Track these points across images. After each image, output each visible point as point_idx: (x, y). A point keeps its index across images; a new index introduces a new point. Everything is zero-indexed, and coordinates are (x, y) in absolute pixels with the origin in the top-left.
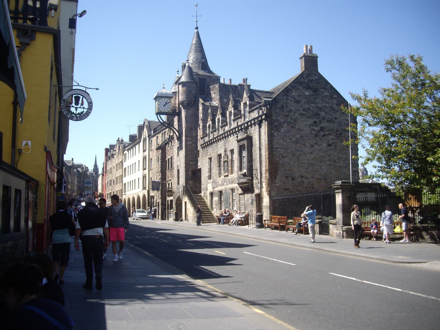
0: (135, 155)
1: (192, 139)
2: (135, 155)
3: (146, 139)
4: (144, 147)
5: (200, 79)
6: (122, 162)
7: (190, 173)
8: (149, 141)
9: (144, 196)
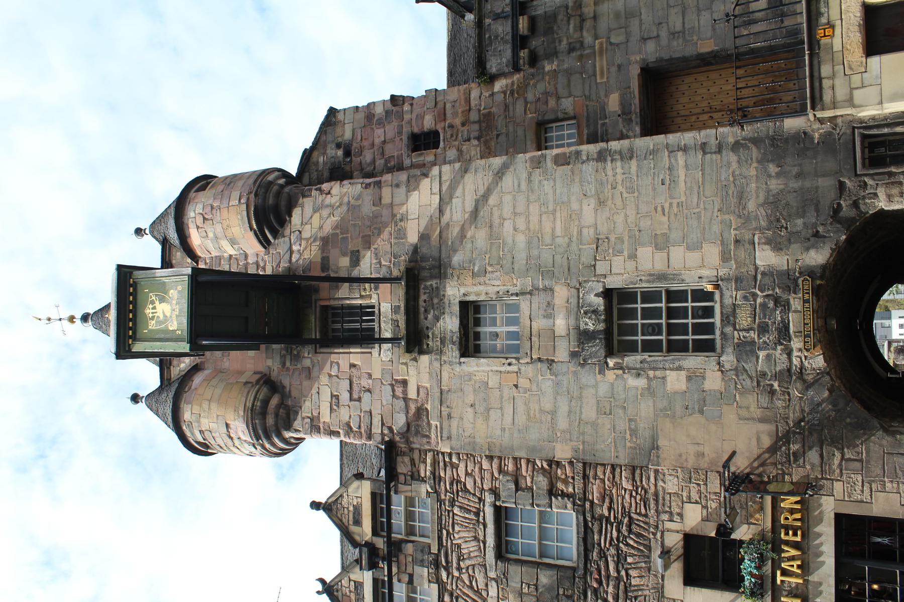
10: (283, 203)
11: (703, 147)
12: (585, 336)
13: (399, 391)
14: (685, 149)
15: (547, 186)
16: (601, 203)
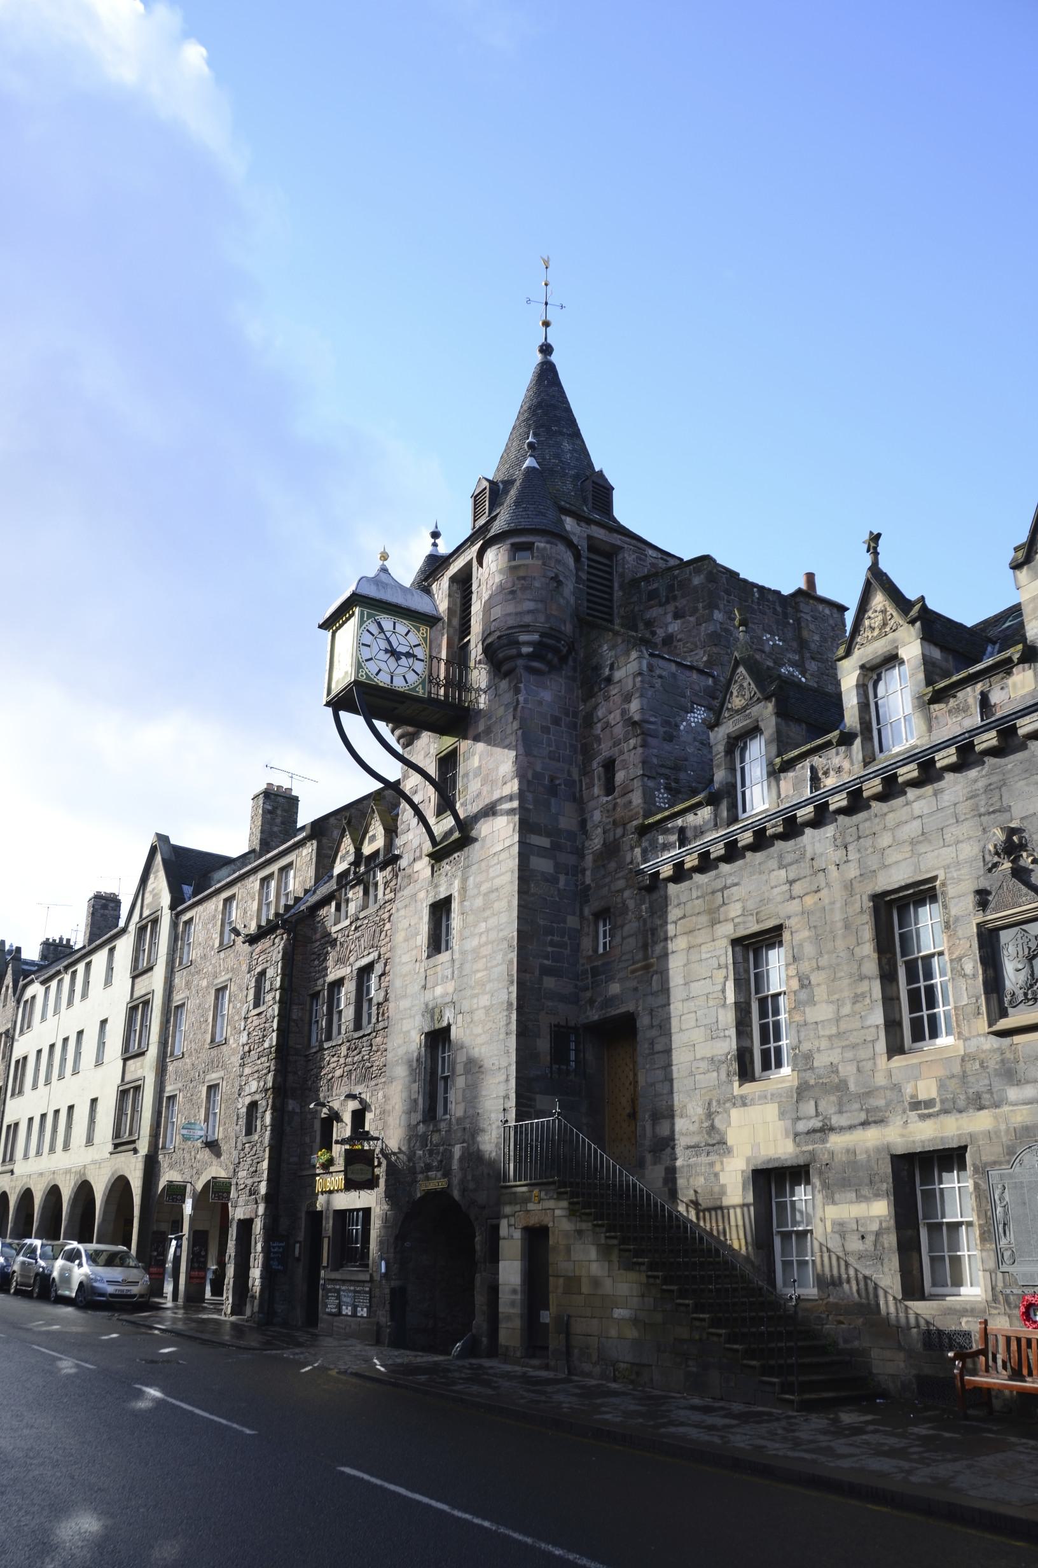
0: (84, 995)
1: (556, 847)
2: (84, 995)
3: (155, 922)
4: (136, 960)
5: (594, 546)
6: (9, 1036)
7: (544, 1045)
8: (174, 924)
9: (120, 1185)
10: (505, 668)
11: (506, 1097)
14: (507, 1080)
15: (499, 957)
16: (487, 1009)
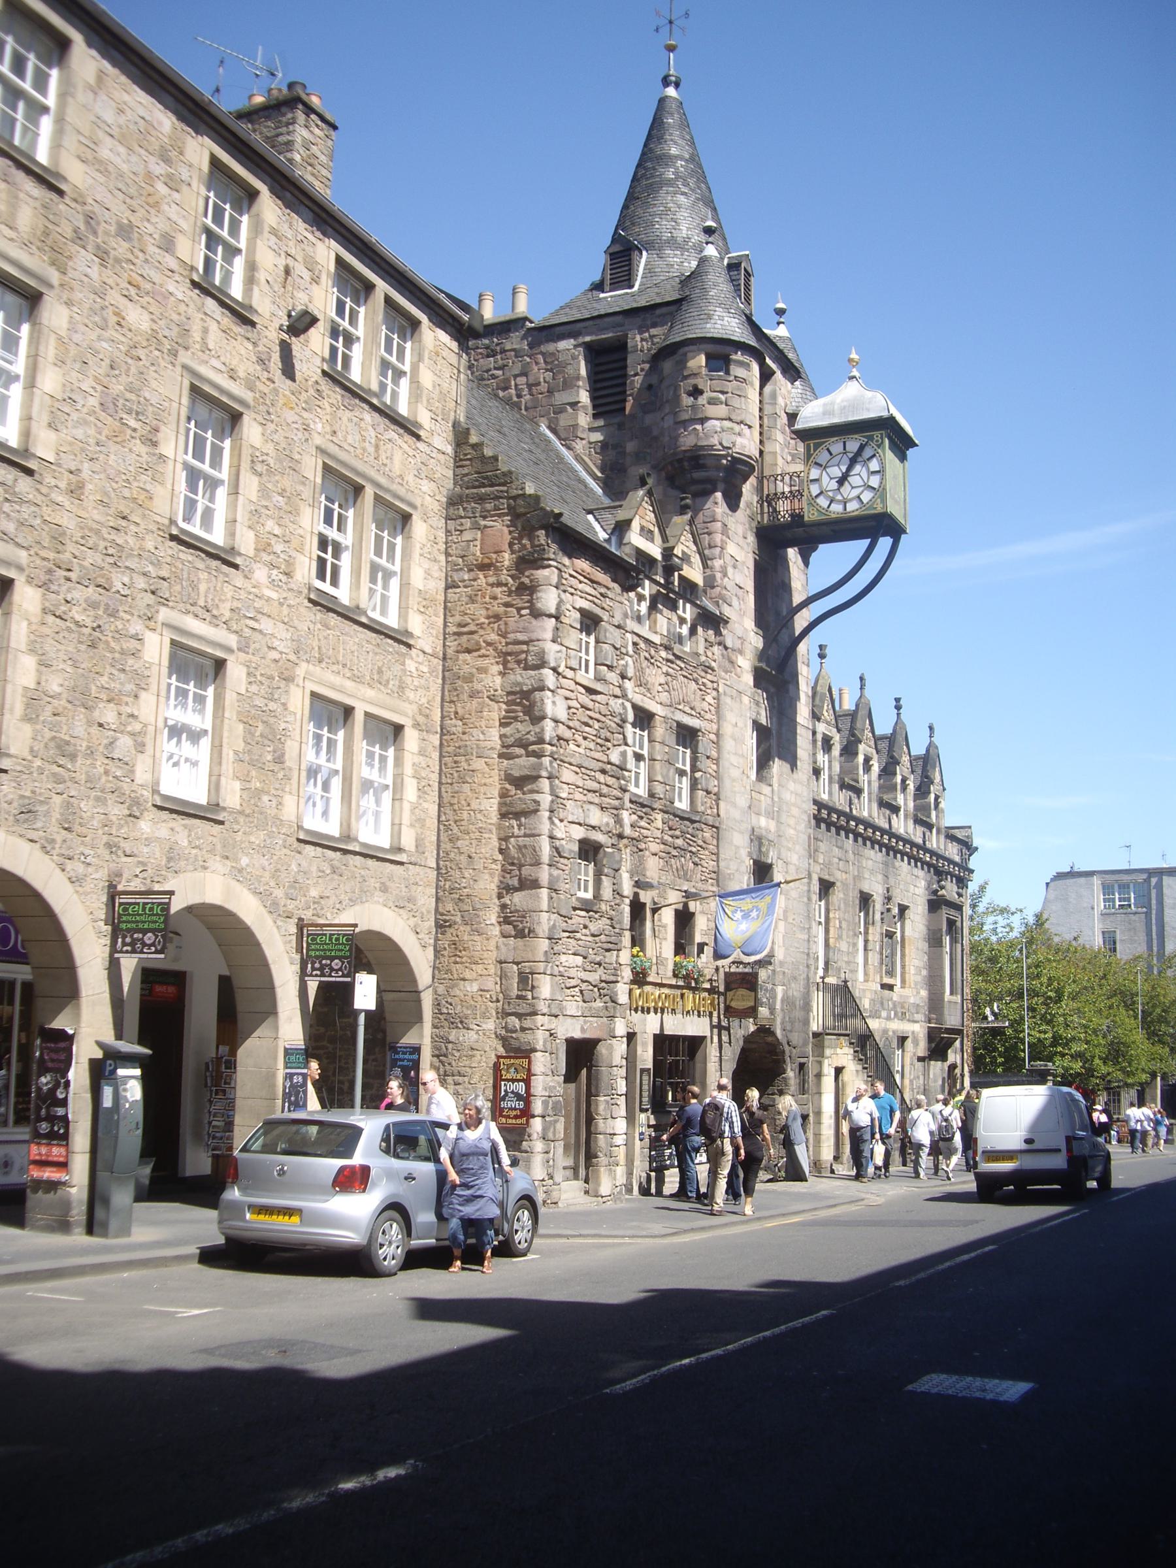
12: (760, 839)
13: (738, 645)
15: (802, 827)
